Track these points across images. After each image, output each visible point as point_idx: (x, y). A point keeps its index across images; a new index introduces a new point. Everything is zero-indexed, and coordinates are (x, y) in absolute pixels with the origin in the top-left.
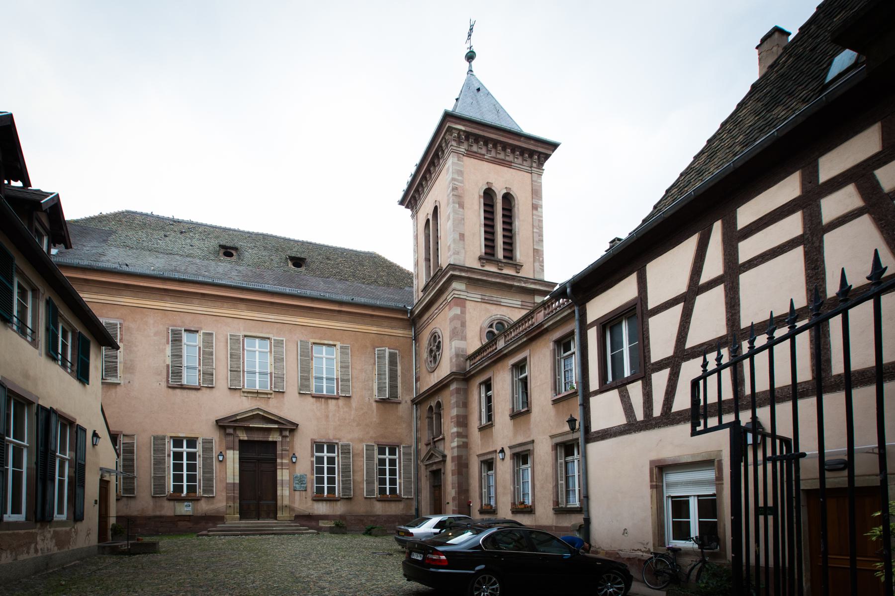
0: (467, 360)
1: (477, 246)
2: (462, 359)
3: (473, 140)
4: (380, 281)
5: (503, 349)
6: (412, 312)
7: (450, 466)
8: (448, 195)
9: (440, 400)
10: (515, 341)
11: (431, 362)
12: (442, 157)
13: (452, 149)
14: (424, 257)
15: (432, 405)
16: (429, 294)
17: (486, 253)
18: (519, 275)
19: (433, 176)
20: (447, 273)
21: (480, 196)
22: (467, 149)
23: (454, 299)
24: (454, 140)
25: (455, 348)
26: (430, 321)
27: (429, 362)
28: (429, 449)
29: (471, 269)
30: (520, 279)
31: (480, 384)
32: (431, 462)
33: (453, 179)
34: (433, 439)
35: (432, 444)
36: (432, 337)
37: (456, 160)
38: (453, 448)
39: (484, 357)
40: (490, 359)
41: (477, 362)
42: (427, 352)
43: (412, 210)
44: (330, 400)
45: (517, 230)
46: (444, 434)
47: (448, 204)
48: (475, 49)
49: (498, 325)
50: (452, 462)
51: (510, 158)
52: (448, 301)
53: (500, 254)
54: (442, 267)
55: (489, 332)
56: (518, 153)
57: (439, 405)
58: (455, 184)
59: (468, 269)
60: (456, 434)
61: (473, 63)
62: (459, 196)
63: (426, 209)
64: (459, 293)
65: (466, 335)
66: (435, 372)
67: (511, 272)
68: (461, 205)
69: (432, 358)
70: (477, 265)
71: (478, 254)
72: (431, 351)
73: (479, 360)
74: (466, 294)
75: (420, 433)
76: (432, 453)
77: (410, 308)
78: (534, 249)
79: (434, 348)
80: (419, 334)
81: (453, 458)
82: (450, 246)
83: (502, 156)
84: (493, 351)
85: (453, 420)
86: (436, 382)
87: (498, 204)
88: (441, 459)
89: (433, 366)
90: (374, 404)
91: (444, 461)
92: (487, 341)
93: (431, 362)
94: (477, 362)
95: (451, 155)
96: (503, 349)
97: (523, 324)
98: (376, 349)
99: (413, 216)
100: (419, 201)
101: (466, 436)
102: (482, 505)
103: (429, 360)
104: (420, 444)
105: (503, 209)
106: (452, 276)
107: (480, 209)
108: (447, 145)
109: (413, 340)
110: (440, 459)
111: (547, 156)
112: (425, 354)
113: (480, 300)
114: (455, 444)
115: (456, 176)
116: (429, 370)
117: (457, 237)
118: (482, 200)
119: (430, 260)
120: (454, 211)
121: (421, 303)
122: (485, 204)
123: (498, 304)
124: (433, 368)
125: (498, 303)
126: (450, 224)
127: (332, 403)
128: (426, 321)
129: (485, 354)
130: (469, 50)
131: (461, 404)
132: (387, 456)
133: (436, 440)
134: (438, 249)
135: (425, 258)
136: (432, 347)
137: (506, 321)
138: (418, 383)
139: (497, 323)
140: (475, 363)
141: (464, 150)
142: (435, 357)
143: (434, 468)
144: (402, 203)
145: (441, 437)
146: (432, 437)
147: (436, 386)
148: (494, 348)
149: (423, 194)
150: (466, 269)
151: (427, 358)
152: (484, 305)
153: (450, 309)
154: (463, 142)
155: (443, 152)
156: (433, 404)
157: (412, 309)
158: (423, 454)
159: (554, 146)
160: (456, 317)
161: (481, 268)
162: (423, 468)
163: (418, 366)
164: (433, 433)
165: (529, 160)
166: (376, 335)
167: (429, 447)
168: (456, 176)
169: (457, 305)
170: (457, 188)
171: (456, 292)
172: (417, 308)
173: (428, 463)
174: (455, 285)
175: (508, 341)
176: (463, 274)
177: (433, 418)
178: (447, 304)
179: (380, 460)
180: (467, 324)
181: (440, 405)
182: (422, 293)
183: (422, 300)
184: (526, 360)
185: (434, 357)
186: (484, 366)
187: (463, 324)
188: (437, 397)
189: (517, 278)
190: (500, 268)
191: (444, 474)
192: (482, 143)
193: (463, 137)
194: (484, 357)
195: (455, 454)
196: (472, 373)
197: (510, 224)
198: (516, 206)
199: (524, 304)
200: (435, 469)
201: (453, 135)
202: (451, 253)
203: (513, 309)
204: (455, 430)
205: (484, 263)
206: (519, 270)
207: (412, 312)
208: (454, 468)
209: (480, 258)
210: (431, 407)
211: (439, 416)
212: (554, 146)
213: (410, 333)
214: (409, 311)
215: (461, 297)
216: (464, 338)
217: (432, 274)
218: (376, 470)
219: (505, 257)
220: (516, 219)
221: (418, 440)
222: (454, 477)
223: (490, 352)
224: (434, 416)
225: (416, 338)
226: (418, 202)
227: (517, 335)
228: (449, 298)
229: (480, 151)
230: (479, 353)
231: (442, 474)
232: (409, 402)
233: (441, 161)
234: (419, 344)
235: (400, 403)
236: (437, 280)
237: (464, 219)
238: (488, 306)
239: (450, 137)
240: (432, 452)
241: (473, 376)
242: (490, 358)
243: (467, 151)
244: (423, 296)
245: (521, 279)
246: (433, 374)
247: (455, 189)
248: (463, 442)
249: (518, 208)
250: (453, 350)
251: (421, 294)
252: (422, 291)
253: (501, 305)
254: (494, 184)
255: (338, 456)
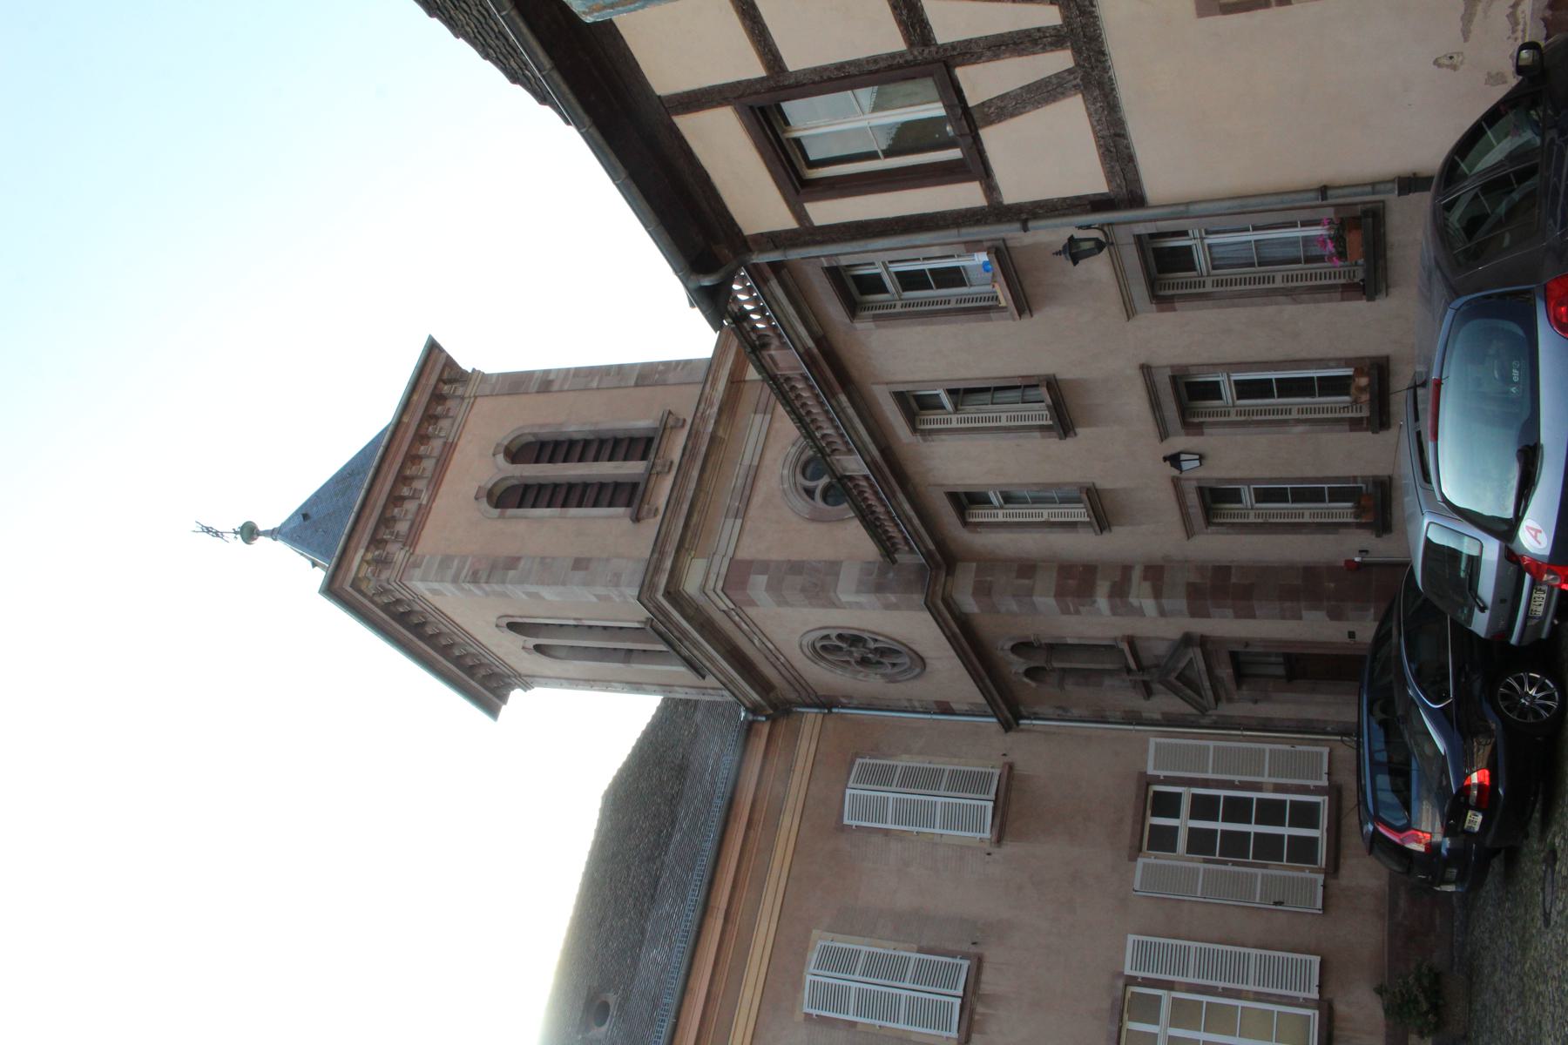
0: (894, 561)
1: (608, 521)
2: (891, 575)
3: (387, 531)
4: (672, 788)
5: (868, 459)
6: (754, 710)
7: (1224, 626)
8: (487, 594)
9: (1009, 645)
10: (848, 425)
11: (894, 665)
12: (408, 606)
13: (395, 581)
14: (621, 665)
15: (1022, 669)
16: (710, 659)
17: (628, 505)
18: (689, 421)
19: (445, 630)
20: (660, 608)
21: (501, 516)
22: (400, 545)
23: (727, 592)
24: (378, 576)
25: (858, 592)
26: (782, 659)
27: (896, 670)
28: (1161, 687)
29: (659, 544)
30: (699, 416)
31: (965, 524)
32: (1207, 684)
33: (455, 580)
34: (1129, 671)
35: (1146, 678)
36: (823, 658)
37: (418, 572)
38: (1162, 613)
39: (889, 513)
40: (894, 496)
41: (901, 531)
42: (866, 676)
43: (511, 687)
44: (982, 986)
45: (587, 428)
46: (1115, 639)
47: (504, 595)
48: (238, 525)
49: (808, 472)
50: (1208, 616)
51: (436, 445)
52: (732, 606)
53: (632, 469)
54: (648, 619)
55: (825, 498)
56: (430, 428)
57: (1022, 647)
58: (466, 577)
59: (658, 550)
60: (1118, 601)
61: (261, 528)
62: (493, 568)
63: (510, 650)
64: (713, 577)
65: (825, 561)
66: (923, 654)
67: (680, 439)
68: (512, 562)
69: (884, 660)
70: (650, 527)
71: (627, 522)
72: (864, 662)
73: (897, 525)
74: (717, 558)
75: (1108, 713)
76: (1178, 678)
77: (743, 714)
78: (637, 385)
79: (857, 653)
80: (817, 697)
81: (1194, 613)
82: (598, 596)
83: (428, 464)
84: (872, 486)
85: (1072, 609)
86: (953, 653)
87: (526, 474)
88: (1198, 651)
89: (907, 660)
90: (1009, 848)
91: (1203, 642)
92: (845, 505)
93: (894, 665)
94: (901, 531)
95: (405, 582)
96: (868, 459)
97: (804, 405)
98: (846, 821)
99: (526, 686)
100: (494, 668)
101: (1126, 569)
102: (1359, 526)
103: (889, 670)
104: (1145, 715)
105: (537, 461)
106: (668, 594)
107: (526, 518)
108: (385, 592)
109: (830, 712)
110: (1195, 654)
111: (450, 363)
112: (870, 683)
113: (739, 522)
114: (1149, 605)
115: (451, 572)
116: (918, 670)
117: (580, 574)
118: (511, 512)
119: (631, 651)
120: (521, 581)
121: (732, 682)
122: (520, 506)
123: (754, 474)
124: (911, 658)
125: (752, 473)
126: (549, 594)
127: (991, 982)
128: (780, 673)
129: (880, 509)
130: (239, 536)
131: (1026, 582)
132: (1184, 823)
133: (1132, 665)
134: (605, 628)
135: (623, 662)
136: (852, 661)
137: (801, 453)
138: (955, 706)
139: (804, 474)
140: (905, 538)
141: (403, 552)
142: (883, 652)
143: (1225, 672)
144: (492, 710)
145: (1125, 647)
146: (1125, 676)
147: (962, 649)
148: (863, 483)
149: (481, 657)
150: (656, 556)
151: (883, 675)
152: (753, 511)
153: (752, 603)
154: (388, 553)
155: (398, 602)
156: (1018, 665)
157: (747, 710)
158: (1176, 705)
159: (433, 348)
160: (774, 587)
161: (659, 517)
162: (1226, 709)
163: (906, 704)
164: (1110, 673)
165: (450, 403)
166: (804, 817)
167: (1157, 687)
168: (451, 572)
169: (743, 584)
170: (473, 573)
171: (711, 583)
172: (745, 695)
173: (1210, 693)
174: (691, 585)
175: (846, 443)
176: (668, 564)
177: (1064, 670)
178: (739, 611)
179: (1191, 849)
180: (795, 558)
181: (1022, 644)
182: (707, 678)
183: (722, 678)
184: (902, 393)
185: (881, 656)
186: (911, 513)
187: (796, 568)
188: (1000, 653)
189: (695, 427)
190: (666, 469)
191: (1247, 645)
192: (396, 510)
193: (377, 553)
194: (889, 513)
195: (1182, 604)
196: (932, 547)
197: (572, 443)
198: (536, 430)
199: (761, 407)
200: (1230, 671)
201: (369, 575)
202: (613, 593)
203: (773, 433)
204: (1102, 603)
205: (650, 510)
206: (678, 419)
207: (754, 710)
208: (1229, 612)
209: (637, 519)
210: (1029, 673)
211: (1056, 648)
212: (433, 348)
213: (811, 717)
214: (750, 717)
215: (724, 570)
216: (833, 567)
217: (662, 647)
218: (1225, 863)
219: (644, 457)
220: (564, 429)
221: (1134, 718)
222: (1257, 613)
223: (876, 493)
224: (1056, 665)
225: (827, 703)
226: (497, 670)
227: (831, 420)
228: (723, 603)
229: (410, 516)
230: (877, 526)
231: (1248, 650)
232: (1012, 737)
233: (417, 608)
234: (844, 697)
235: (1011, 767)
236: (676, 634)
237: (543, 558)
238: (757, 500)
239: (372, 584)
240: (1172, 678)
241: (941, 544)
242: (891, 496)
243: (404, 545)
244: (714, 675)
245: (699, 415)
246: (927, 661)
247: (475, 578)
248: (1145, 578)
249: (542, 426)
250: (863, 599)
251: (710, 681)
252: (704, 677)
253: (758, 467)
254: (482, 484)
255: (1169, 985)
